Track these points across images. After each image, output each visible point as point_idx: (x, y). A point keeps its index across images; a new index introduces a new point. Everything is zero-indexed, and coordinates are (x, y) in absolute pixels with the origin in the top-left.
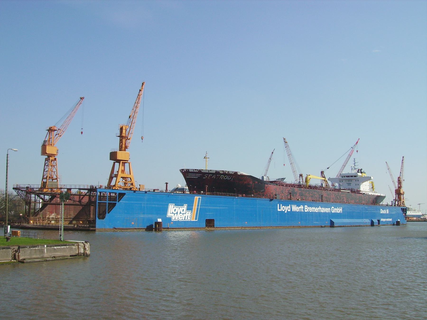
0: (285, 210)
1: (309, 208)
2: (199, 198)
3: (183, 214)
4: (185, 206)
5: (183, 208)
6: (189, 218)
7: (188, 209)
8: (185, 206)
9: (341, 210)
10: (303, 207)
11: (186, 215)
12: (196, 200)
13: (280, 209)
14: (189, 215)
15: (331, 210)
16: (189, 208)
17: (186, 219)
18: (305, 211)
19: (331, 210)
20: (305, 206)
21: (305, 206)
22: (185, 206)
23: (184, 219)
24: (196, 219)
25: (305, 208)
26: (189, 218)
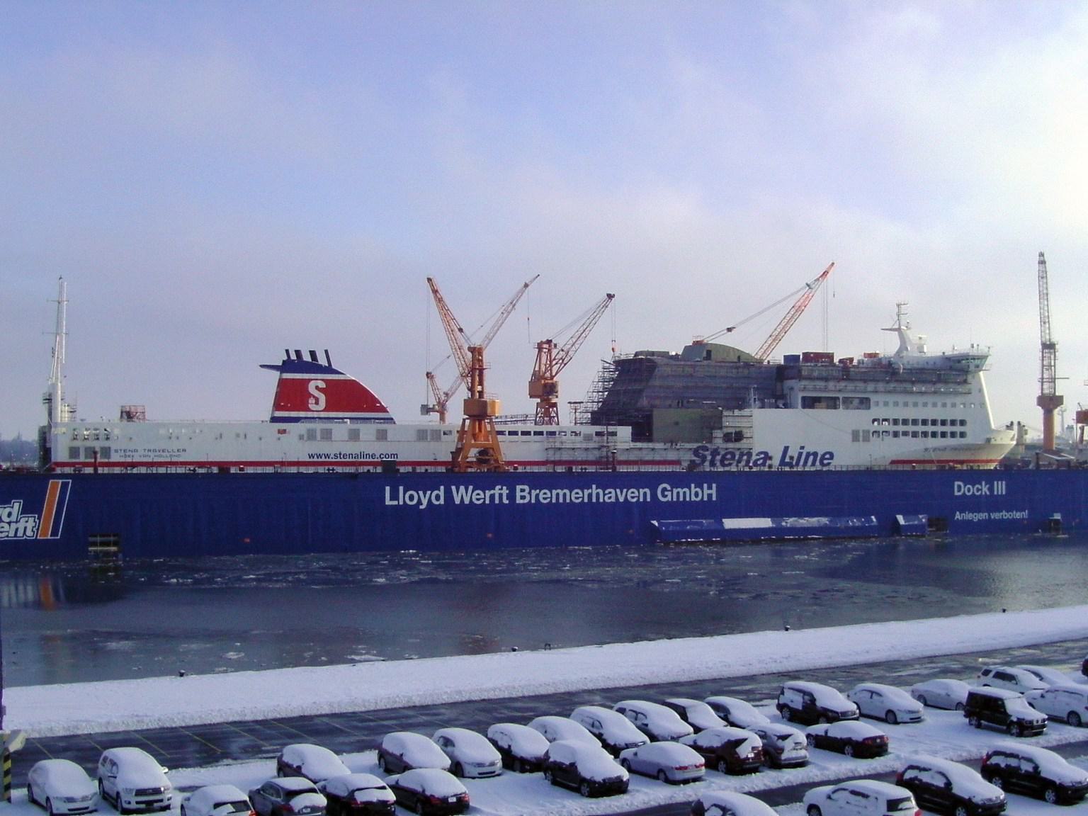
0: (420, 502)
1: (534, 493)
2: (65, 485)
3: (9, 523)
4: (17, 506)
5: (8, 510)
6: (29, 533)
7: (25, 511)
8: (16, 505)
9: (714, 492)
10: (505, 491)
11: (21, 525)
12: (54, 488)
13: (645, 494)
14: (31, 524)
15: (654, 495)
16: (33, 507)
17: (20, 533)
18: (519, 501)
19: (654, 495)
20: (518, 488)
21: (518, 488)
22: (17, 506)
23: (12, 534)
24: (54, 533)
25: (518, 494)
26: (29, 533)
